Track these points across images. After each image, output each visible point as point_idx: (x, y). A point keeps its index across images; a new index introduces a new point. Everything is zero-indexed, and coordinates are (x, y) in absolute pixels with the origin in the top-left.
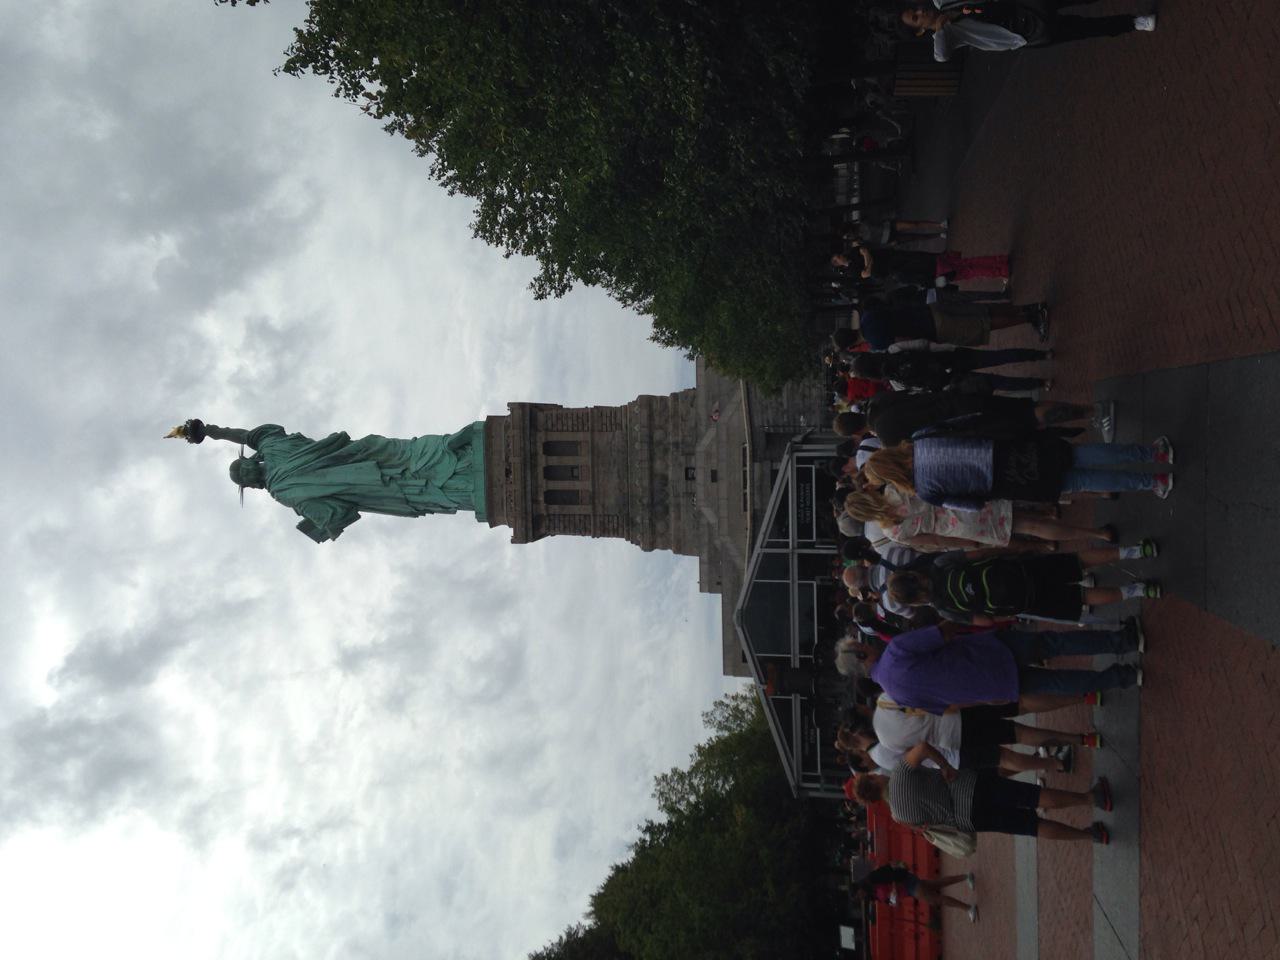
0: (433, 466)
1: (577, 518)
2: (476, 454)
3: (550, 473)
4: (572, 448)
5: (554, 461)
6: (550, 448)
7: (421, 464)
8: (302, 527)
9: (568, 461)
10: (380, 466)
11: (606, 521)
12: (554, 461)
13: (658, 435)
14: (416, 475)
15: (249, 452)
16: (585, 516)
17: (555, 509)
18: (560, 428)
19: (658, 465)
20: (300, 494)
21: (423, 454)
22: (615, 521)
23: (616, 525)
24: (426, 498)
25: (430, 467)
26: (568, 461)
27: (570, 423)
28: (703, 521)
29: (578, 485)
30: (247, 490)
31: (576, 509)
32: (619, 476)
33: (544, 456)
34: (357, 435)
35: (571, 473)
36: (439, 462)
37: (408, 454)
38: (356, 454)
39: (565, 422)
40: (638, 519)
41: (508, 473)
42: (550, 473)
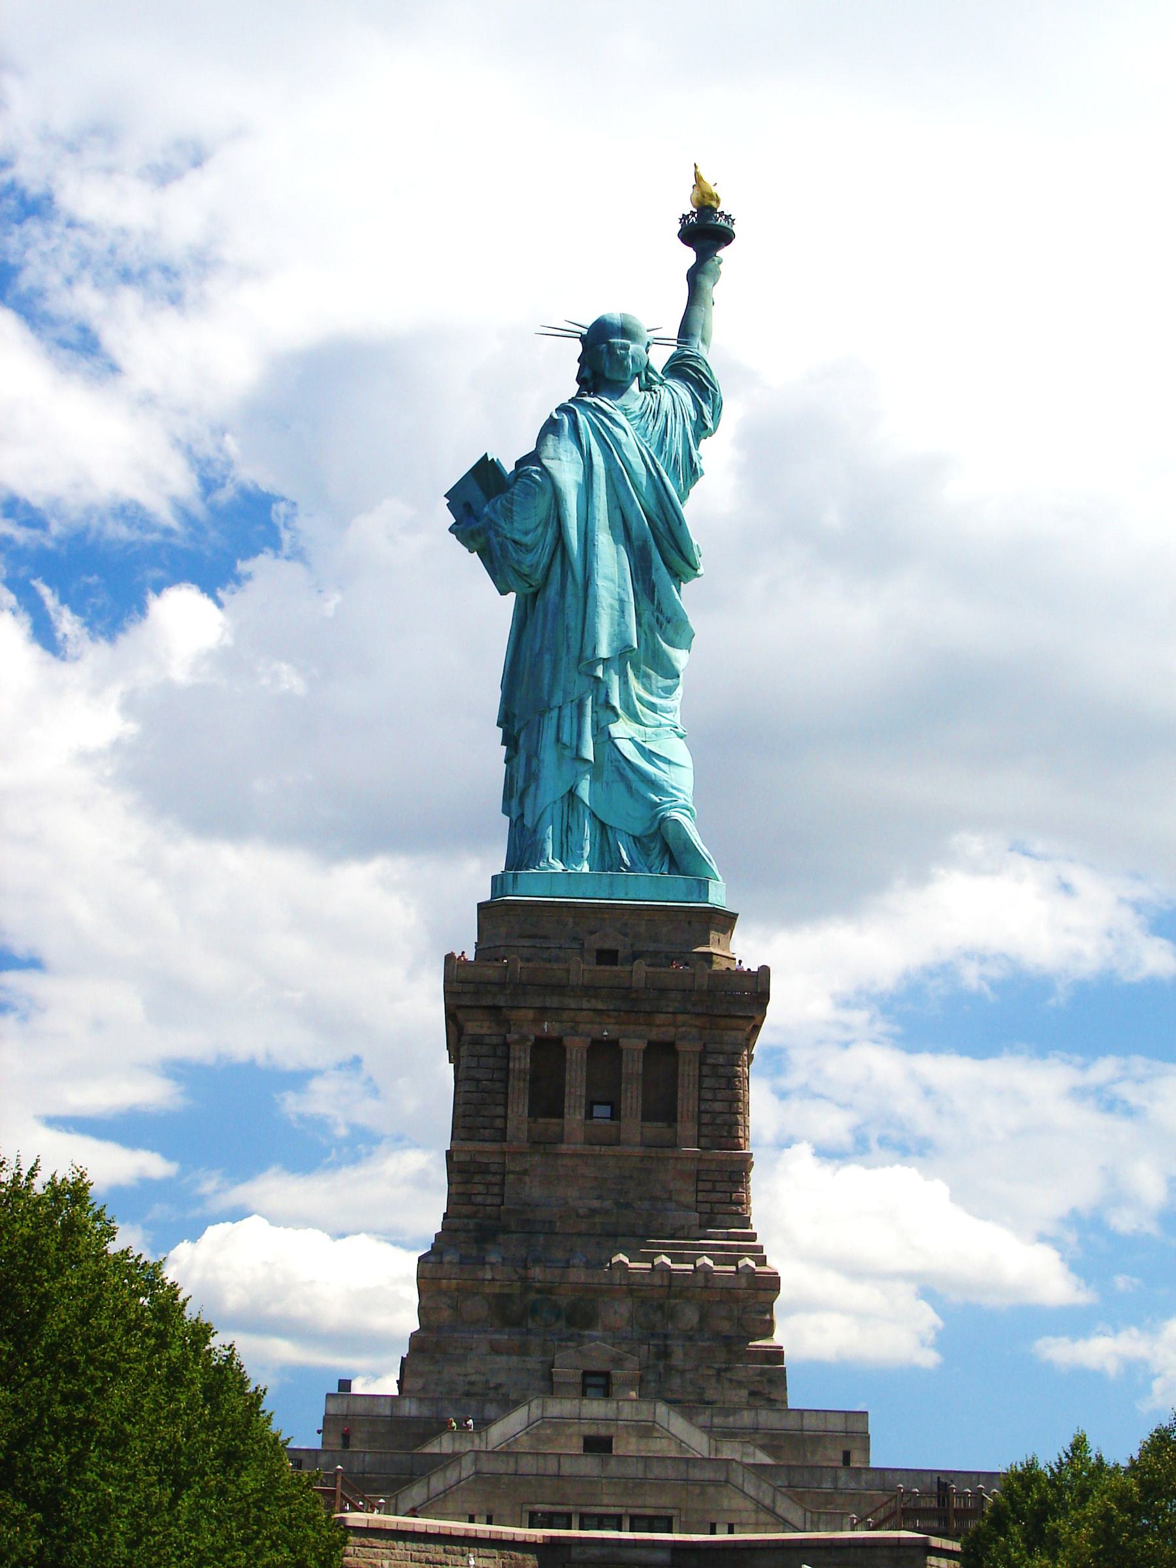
0: (623, 777)
1: (500, 1110)
5: (633, 1066)
9: (632, 1099)
11: (489, 1178)
12: (633, 1066)
15: (659, 358)
16: (504, 1130)
18: (707, 1082)
22: (489, 1200)
23: (479, 1199)
26: (632, 1099)
27: (718, 1106)
29: (574, 1117)
30: (577, 348)
31: (519, 1110)
32: (593, 1212)
33: (641, 1044)
36: (629, 788)
38: (652, 601)
39: (720, 1096)
41: (607, 957)
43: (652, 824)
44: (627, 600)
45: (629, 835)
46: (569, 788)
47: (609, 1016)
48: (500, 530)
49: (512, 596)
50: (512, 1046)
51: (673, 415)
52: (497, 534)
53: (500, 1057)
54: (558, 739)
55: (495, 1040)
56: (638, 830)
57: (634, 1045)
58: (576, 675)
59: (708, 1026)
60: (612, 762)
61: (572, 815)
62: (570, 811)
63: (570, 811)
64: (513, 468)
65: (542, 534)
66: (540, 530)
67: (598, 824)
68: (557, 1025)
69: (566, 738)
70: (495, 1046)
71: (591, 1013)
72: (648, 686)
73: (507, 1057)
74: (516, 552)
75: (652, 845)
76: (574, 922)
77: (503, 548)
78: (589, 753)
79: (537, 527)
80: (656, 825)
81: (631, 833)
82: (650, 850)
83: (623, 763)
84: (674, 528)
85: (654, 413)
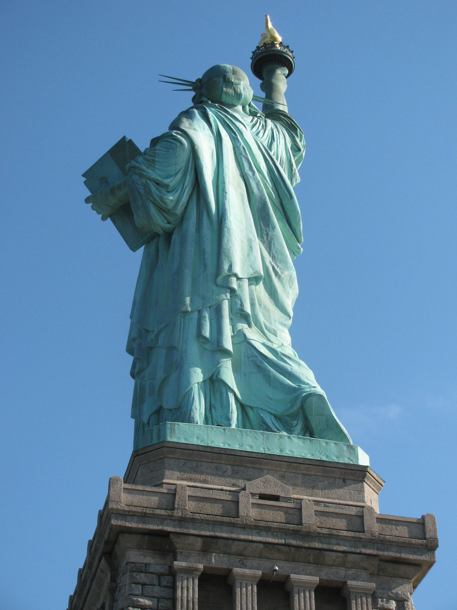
43: (292, 406)
44: (253, 239)
45: (271, 414)
46: (210, 375)
47: (279, 551)
48: (144, 173)
49: (141, 250)
50: (179, 576)
51: (277, 132)
52: (141, 176)
53: (165, 587)
54: (199, 335)
55: (159, 569)
56: (279, 409)
58: (214, 287)
59: (376, 573)
60: (248, 358)
61: (214, 397)
62: (212, 394)
63: (212, 394)
64: (148, 146)
65: (181, 180)
66: (179, 176)
67: (239, 405)
68: (225, 558)
69: (207, 333)
70: (160, 575)
71: (262, 546)
72: (268, 319)
73: (174, 588)
74: (158, 189)
75: (295, 422)
76: (233, 470)
77: (146, 187)
78: (228, 344)
79: (177, 174)
80: (298, 403)
81: (273, 412)
82: (293, 427)
83: (260, 358)
84: (284, 202)
85: (263, 126)
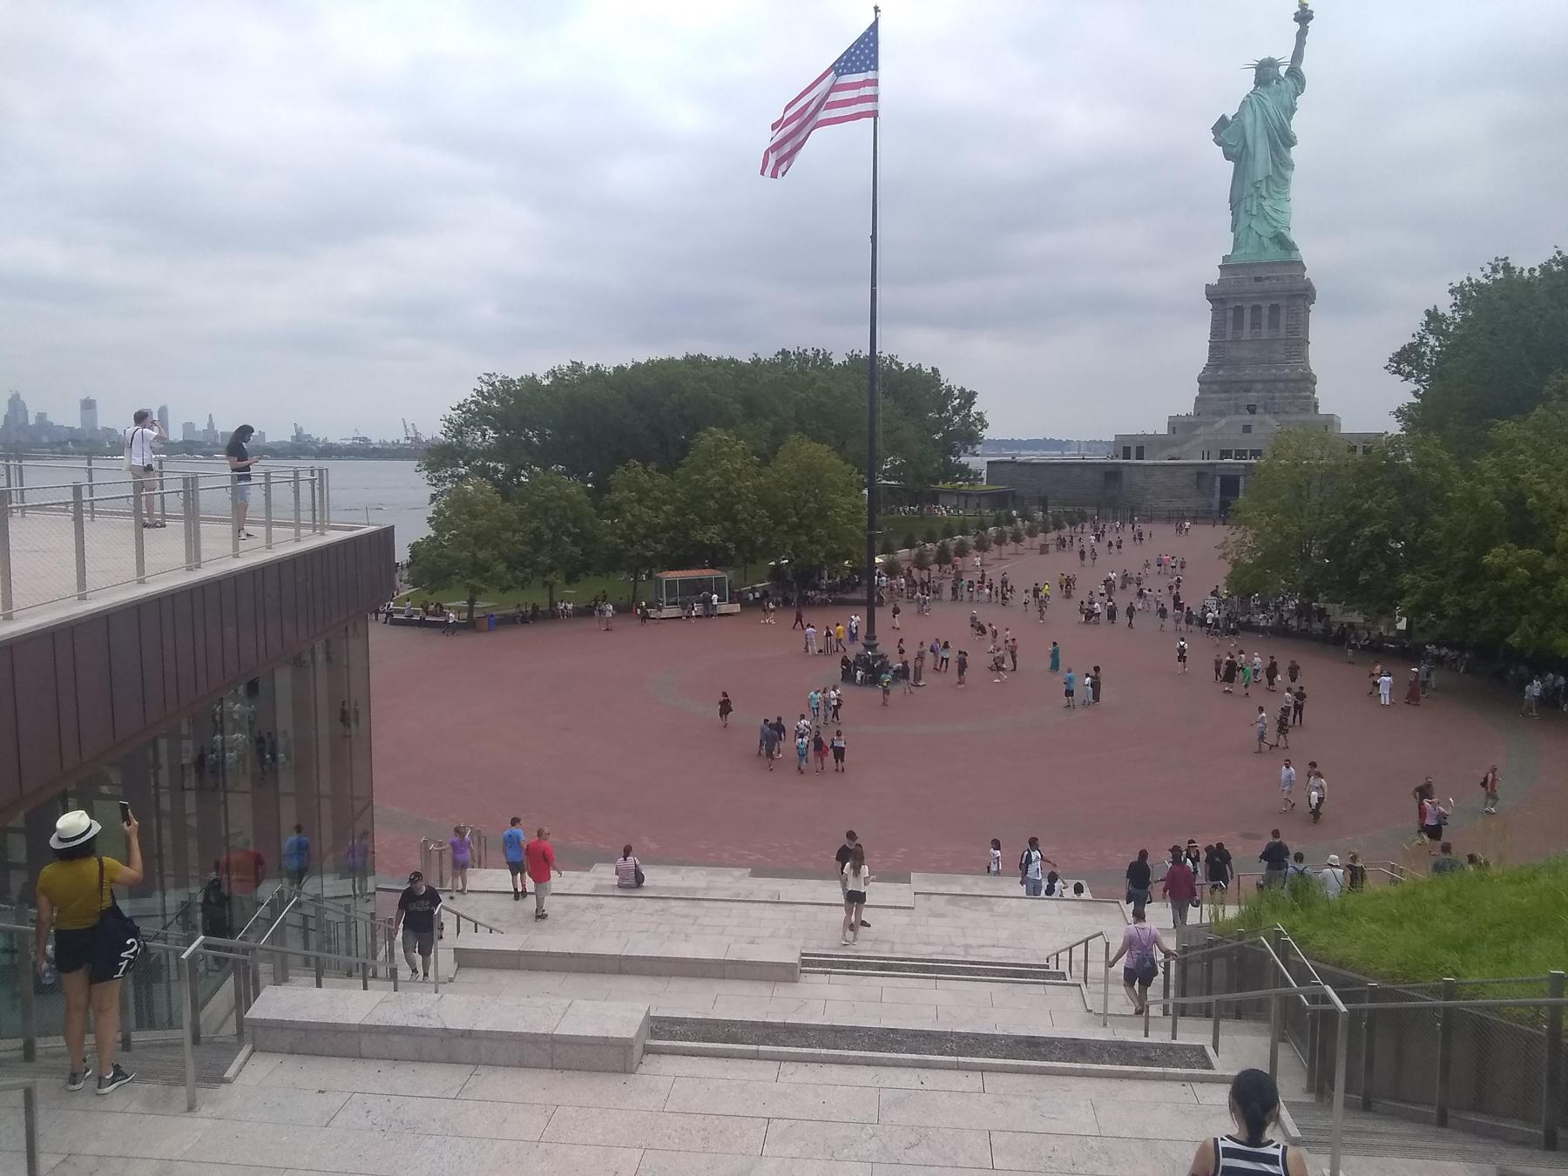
2: (1273, 253)
3: (1256, 309)
4: (1274, 324)
5: (1265, 312)
6: (1274, 309)
7: (1268, 209)
8: (1223, 118)
9: (1265, 322)
10: (1268, 177)
12: (1265, 312)
13: (1281, 385)
14: (1260, 206)
17: (1230, 314)
19: (1260, 386)
20: (1248, 120)
21: (1276, 211)
24: (1242, 215)
25: (1265, 217)
26: (1265, 322)
28: (1217, 419)
34: (1295, 153)
35: (1256, 324)
36: (1269, 223)
37: (1277, 196)
40: (1221, 372)
41: (1258, 279)
42: (1256, 309)
57: (1265, 305)
